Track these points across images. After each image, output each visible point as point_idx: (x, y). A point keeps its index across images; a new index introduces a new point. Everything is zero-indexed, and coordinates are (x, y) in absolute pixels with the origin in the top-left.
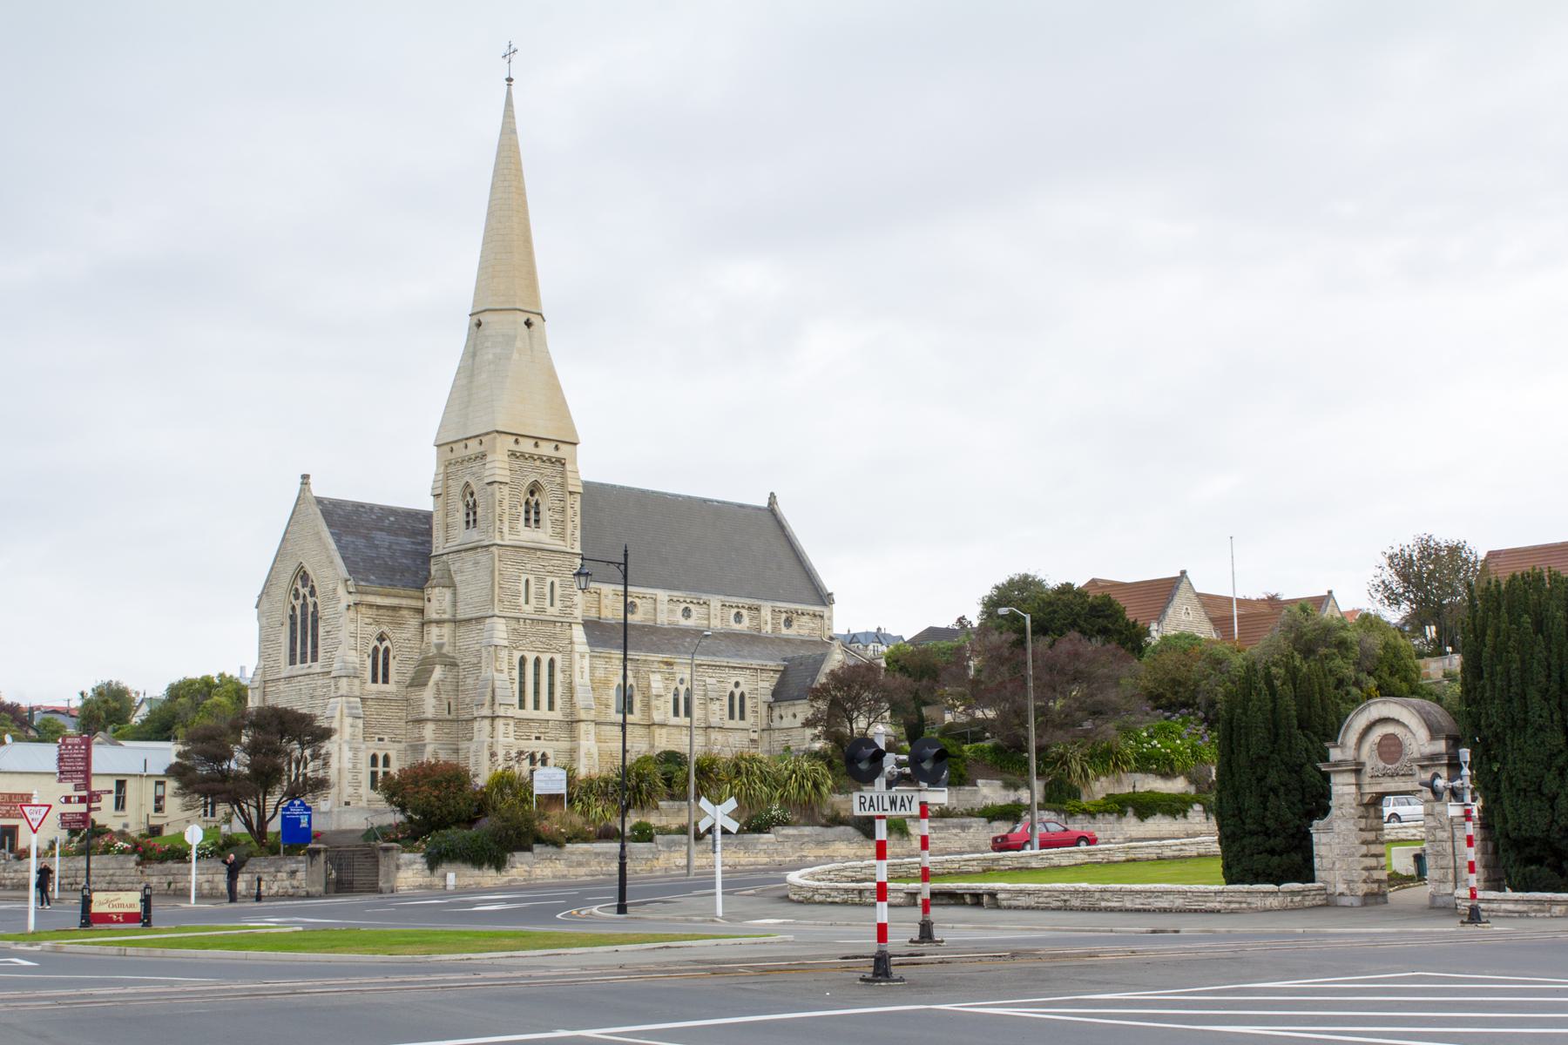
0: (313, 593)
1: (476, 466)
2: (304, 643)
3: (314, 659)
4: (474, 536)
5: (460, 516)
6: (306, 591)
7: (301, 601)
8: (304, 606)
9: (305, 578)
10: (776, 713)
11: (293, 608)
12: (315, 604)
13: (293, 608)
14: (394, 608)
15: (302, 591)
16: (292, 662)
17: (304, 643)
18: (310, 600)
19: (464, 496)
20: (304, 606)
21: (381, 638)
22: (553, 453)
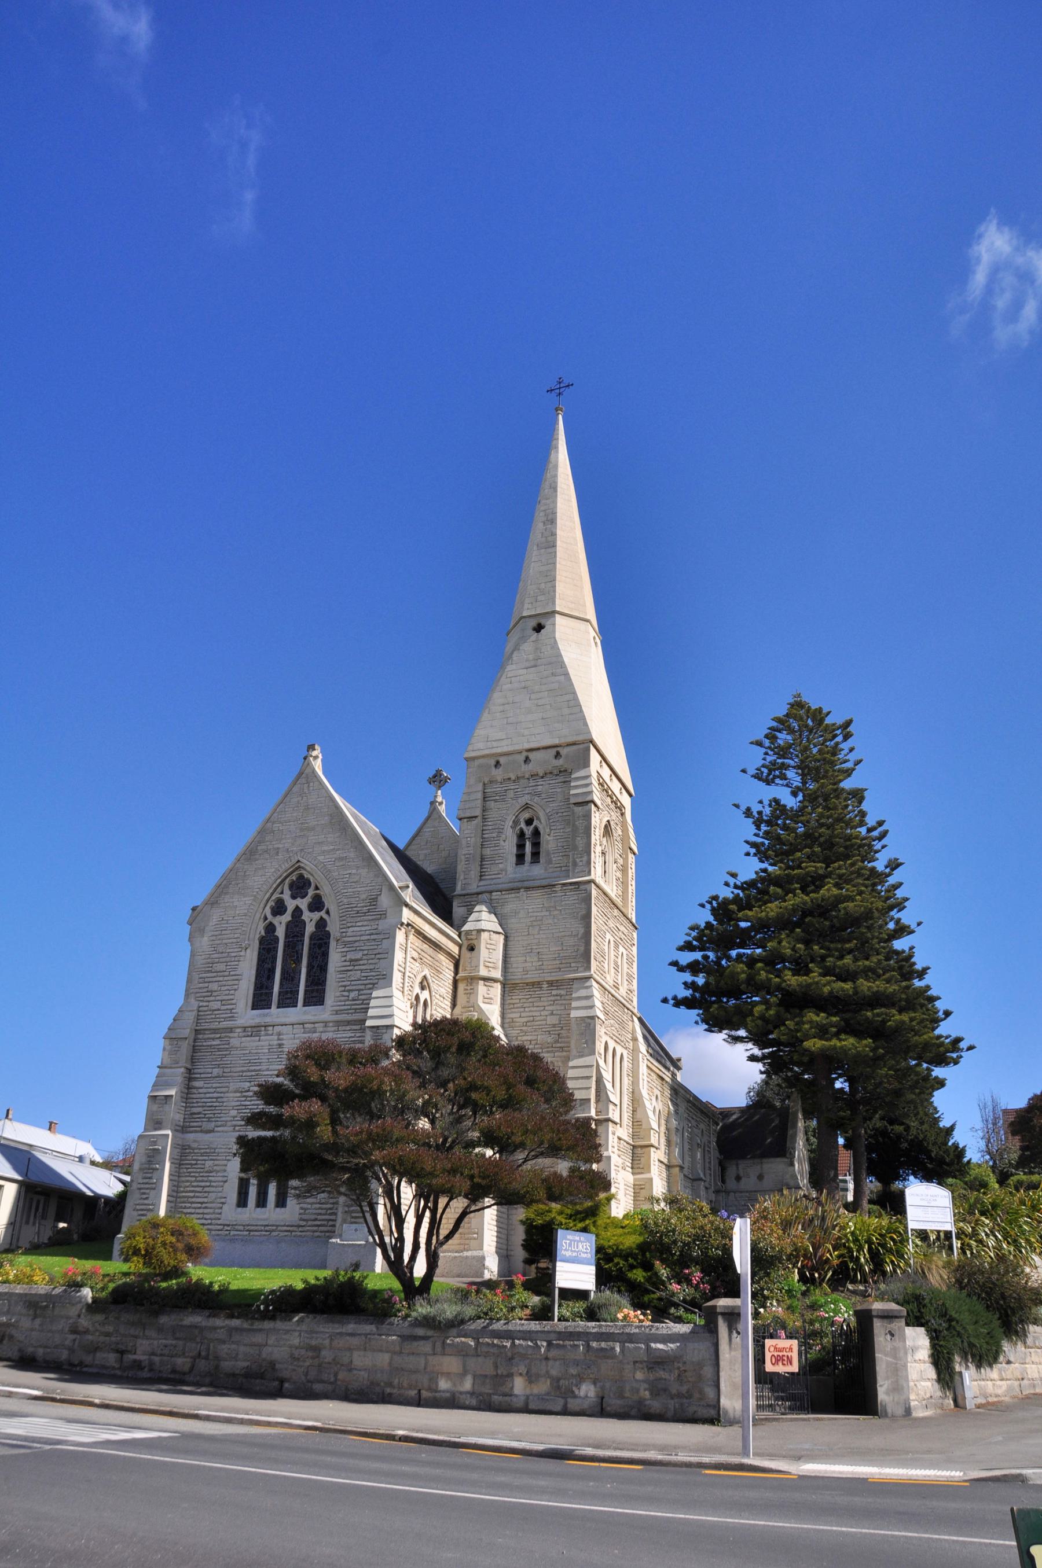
0: (317, 904)
1: (543, 786)
2: (290, 977)
3: (316, 996)
4: (537, 870)
5: (509, 846)
6: (303, 903)
7: (287, 917)
8: (296, 924)
9: (300, 886)
10: (731, 1172)
11: (270, 928)
12: (321, 924)
13: (270, 928)
14: (436, 946)
15: (291, 904)
16: (261, 1000)
17: (290, 977)
18: (310, 919)
19: (516, 823)
20: (296, 924)
21: (423, 988)
22: (617, 792)
